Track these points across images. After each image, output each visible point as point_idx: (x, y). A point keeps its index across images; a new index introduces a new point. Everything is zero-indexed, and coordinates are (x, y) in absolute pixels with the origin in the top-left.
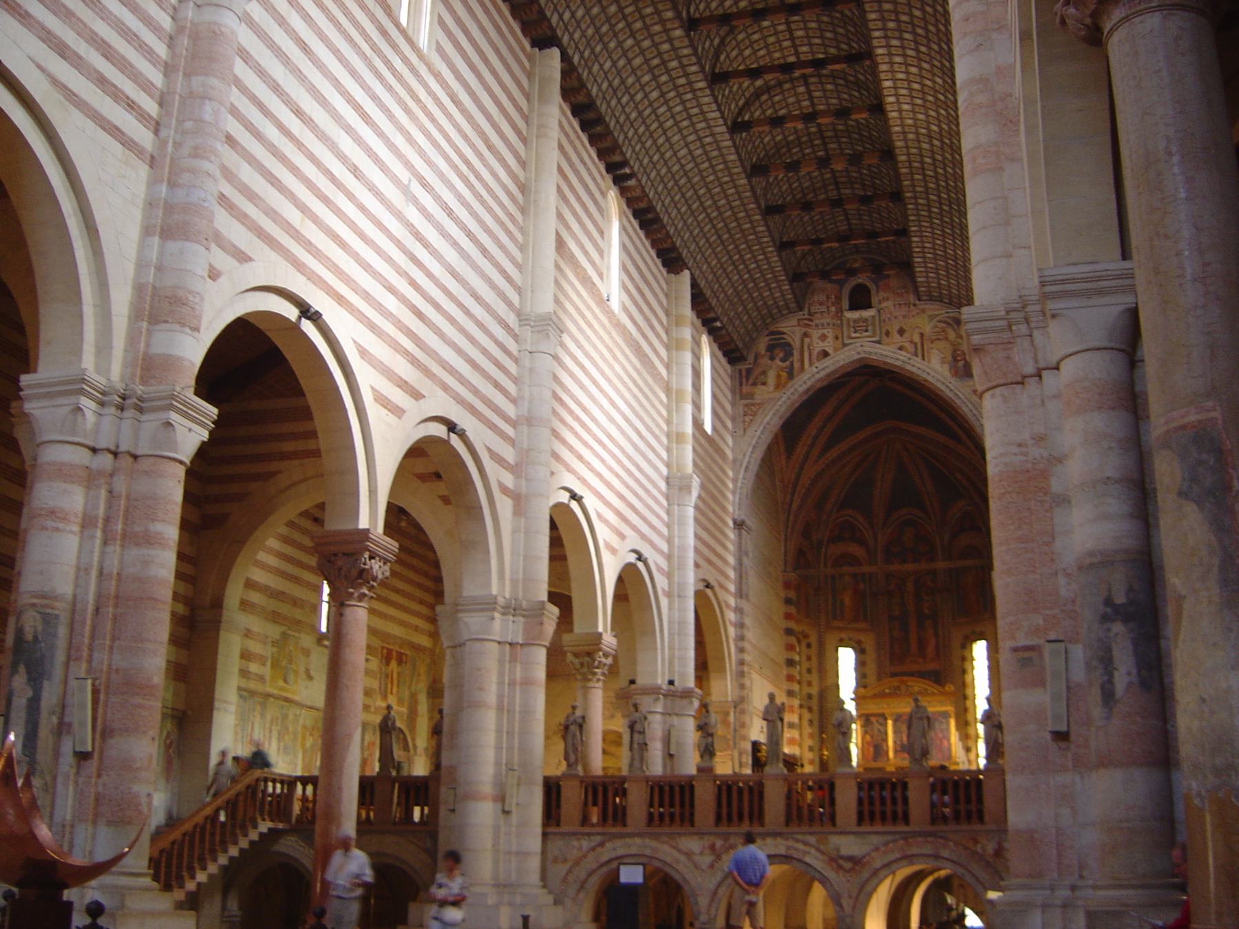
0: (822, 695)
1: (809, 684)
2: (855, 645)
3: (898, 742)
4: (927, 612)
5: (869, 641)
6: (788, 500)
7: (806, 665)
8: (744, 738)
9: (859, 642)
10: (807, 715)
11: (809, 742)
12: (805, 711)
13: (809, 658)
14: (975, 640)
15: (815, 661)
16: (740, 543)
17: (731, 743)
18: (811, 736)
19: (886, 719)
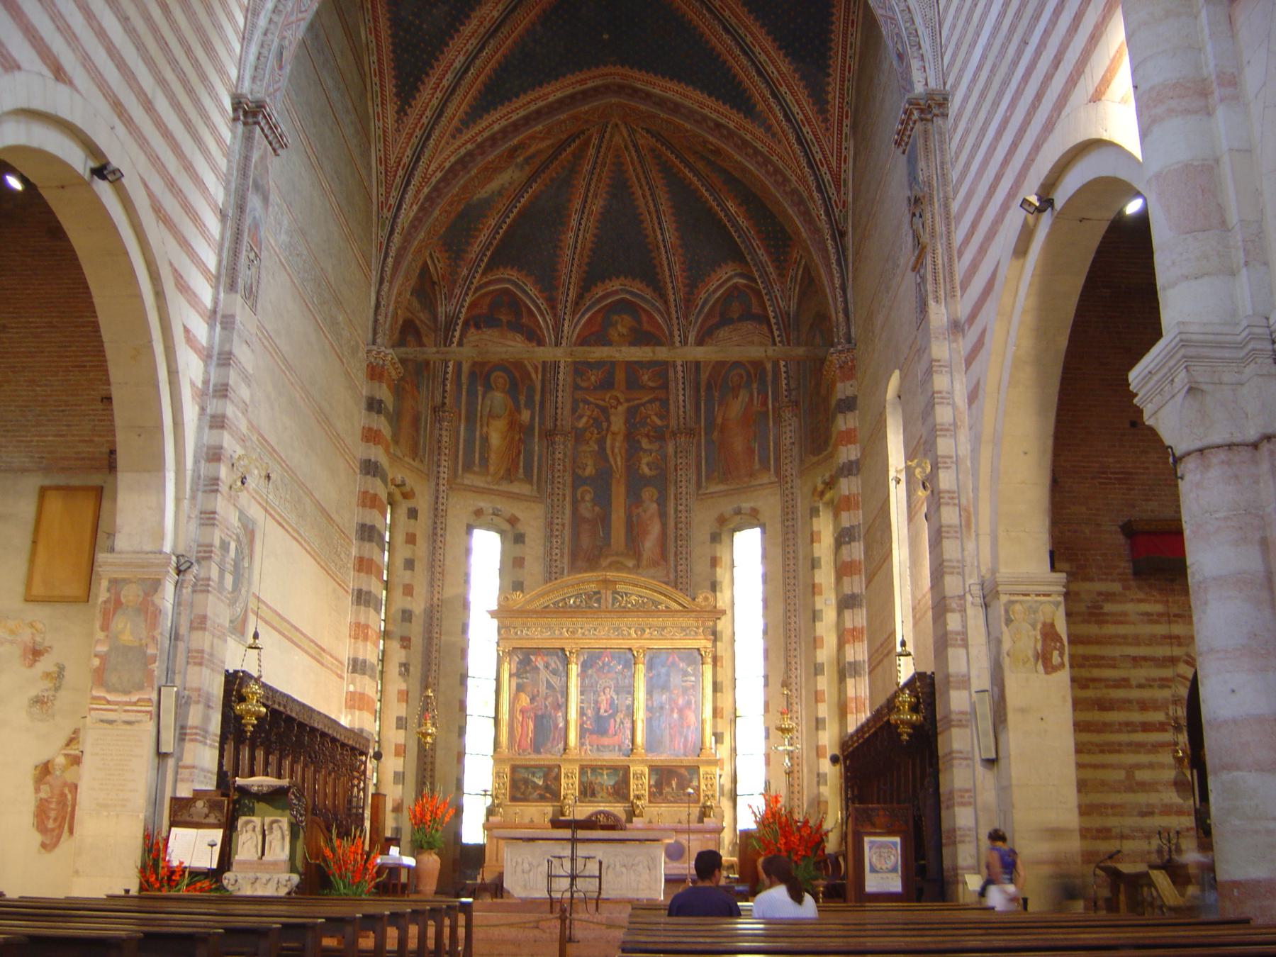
0: (432, 614)
1: (408, 590)
2: (507, 526)
3: (590, 713)
4: (646, 470)
5: (532, 519)
6: (392, 201)
7: (403, 552)
8: (198, 658)
9: (513, 521)
10: (398, 654)
11: (397, 709)
12: (395, 645)
13: (411, 539)
14: (739, 528)
15: (422, 547)
16: (247, 158)
17: (158, 668)
18: (404, 696)
19: (566, 662)
